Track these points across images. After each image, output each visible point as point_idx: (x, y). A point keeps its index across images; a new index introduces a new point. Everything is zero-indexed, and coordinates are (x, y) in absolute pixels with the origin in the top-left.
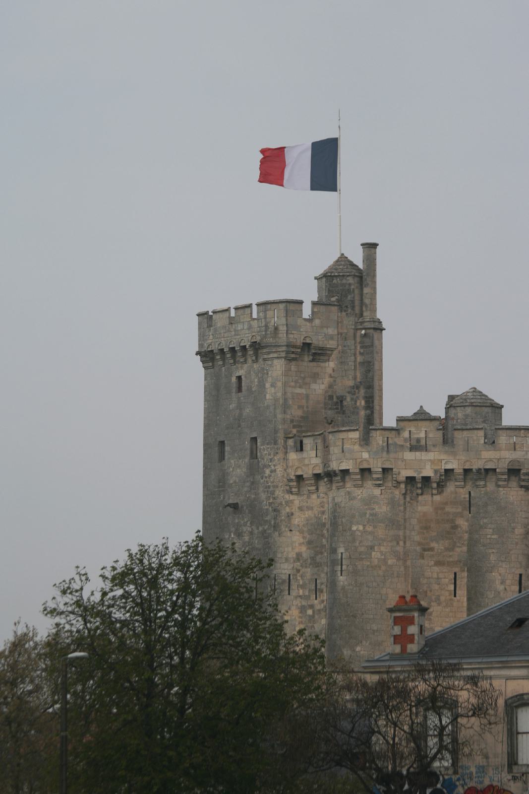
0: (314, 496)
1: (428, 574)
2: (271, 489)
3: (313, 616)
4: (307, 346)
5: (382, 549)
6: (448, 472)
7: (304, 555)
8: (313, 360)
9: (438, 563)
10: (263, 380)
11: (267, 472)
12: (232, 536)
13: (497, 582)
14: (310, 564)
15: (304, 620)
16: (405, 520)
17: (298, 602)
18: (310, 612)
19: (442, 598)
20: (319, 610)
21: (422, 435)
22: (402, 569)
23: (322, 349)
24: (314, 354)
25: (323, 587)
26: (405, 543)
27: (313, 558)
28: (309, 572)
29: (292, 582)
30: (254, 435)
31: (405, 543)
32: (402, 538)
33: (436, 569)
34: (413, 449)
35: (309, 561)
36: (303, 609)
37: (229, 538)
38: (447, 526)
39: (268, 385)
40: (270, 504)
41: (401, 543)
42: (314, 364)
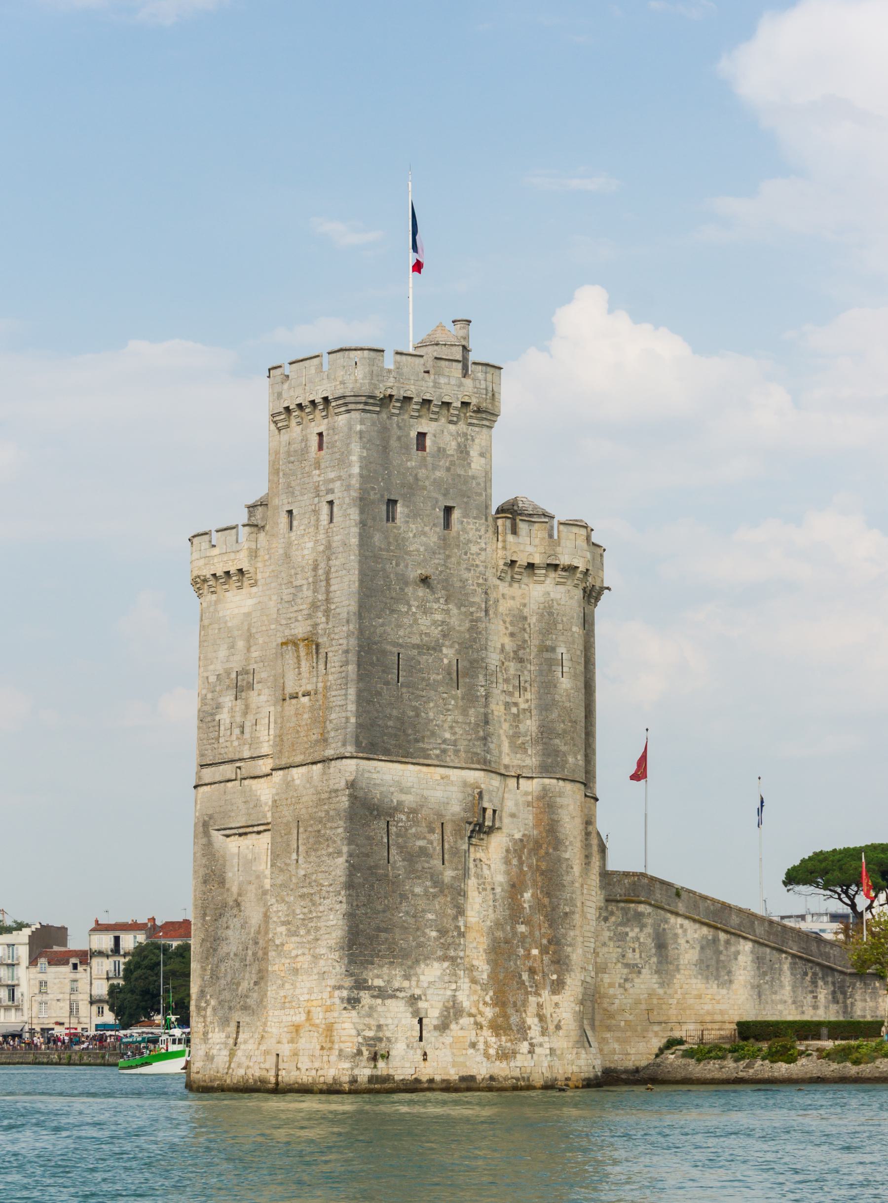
0: (516, 585)
2: (481, 569)
3: (518, 715)
7: (507, 648)
10: (465, 446)
11: (474, 549)
12: (414, 610)
14: (514, 658)
15: (508, 717)
17: (503, 697)
18: (514, 710)
20: (524, 710)
25: (527, 685)
27: (515, 652)
28: (512, 667)
29: (499, 675)
30: (450, 504)
35: (512, 654)
36: (507, 705)
37: (407, 612)
39: (472, 453)
40: (479, 585)
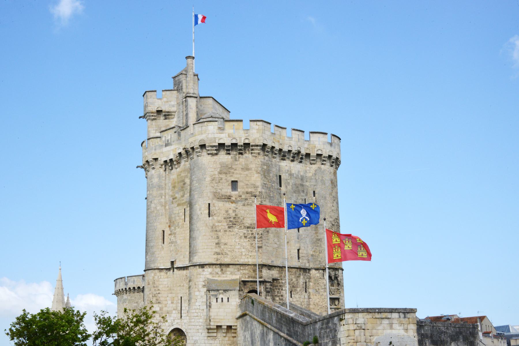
1: (175, 212)
4: (159, 112)
5: (155, 201)
6: (180, 154)
8: (166, 119)
9: (179, 205)
13: (198, 210)
16: (165, 184)
19: (180, 224)
21: (169, 137)
22: (164, 211)
23: (168, 112)
24: (165, 115)
26: (165, 196)
31: (165, 196)
32: (164, 194)
33: (178, 208)
34: (166, 145)
38: (182, 184)
41: (163, 197)
42: (167, 120)
